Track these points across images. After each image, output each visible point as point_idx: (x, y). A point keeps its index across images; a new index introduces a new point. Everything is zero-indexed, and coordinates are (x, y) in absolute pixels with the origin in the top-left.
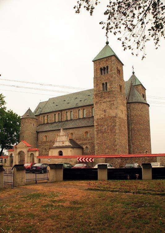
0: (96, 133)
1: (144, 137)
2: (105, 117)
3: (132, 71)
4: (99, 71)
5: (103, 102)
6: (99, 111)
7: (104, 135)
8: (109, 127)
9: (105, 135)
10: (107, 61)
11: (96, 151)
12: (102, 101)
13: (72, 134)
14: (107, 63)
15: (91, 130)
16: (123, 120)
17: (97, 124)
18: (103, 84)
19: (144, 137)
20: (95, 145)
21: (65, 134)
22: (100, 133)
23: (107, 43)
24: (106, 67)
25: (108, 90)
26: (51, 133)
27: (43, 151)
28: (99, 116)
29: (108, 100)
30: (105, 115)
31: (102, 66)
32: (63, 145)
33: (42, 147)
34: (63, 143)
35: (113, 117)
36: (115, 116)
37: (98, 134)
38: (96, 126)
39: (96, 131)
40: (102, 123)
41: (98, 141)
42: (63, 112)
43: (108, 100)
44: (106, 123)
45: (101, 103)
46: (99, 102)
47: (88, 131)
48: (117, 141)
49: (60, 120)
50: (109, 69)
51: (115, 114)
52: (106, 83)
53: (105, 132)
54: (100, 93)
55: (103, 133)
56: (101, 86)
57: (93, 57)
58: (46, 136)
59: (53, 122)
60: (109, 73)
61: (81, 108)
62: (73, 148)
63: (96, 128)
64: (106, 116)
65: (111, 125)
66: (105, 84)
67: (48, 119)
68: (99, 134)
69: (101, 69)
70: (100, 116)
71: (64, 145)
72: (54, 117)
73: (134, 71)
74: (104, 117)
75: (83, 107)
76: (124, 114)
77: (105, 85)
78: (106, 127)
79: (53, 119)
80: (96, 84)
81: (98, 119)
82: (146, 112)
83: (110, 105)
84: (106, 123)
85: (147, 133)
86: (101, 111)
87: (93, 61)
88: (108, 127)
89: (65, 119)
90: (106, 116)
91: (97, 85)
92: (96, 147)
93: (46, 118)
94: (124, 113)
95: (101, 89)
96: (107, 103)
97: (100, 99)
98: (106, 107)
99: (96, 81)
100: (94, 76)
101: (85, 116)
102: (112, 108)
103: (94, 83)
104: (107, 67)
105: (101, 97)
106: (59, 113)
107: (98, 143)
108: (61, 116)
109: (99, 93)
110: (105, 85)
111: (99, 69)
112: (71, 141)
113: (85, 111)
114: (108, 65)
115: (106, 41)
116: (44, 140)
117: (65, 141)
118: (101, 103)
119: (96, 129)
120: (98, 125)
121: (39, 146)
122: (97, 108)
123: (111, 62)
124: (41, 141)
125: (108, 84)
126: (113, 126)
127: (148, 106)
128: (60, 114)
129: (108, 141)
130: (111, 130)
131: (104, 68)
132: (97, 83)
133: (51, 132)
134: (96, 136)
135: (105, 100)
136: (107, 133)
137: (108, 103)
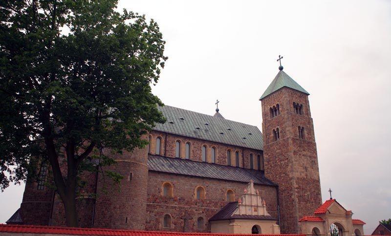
9: (308, 204)
10: (300, 97)
15: (264, 191)
17: (297, 186)
18: (299, 127)
23: (281, 68)
26: (182, 181)
29: (309, 154)
30: (306, 175)
33: (156, 210)
38: (297, 188)
42: (170, 139)
55: (306, 202)
61: (209, 144)
65: (314, 191)
74: (305, 177)
75: (215, 144)
77: (301, 130)
88: (311, 194)
105: (300, 146)
108: (166, 144)
110: (301, 130)
116: (162, 194)
117: (260, 206)
119: (297, 194)
124: (153, 196)
126: (317, 194)
133: (183, 177)
135: (305, 153)
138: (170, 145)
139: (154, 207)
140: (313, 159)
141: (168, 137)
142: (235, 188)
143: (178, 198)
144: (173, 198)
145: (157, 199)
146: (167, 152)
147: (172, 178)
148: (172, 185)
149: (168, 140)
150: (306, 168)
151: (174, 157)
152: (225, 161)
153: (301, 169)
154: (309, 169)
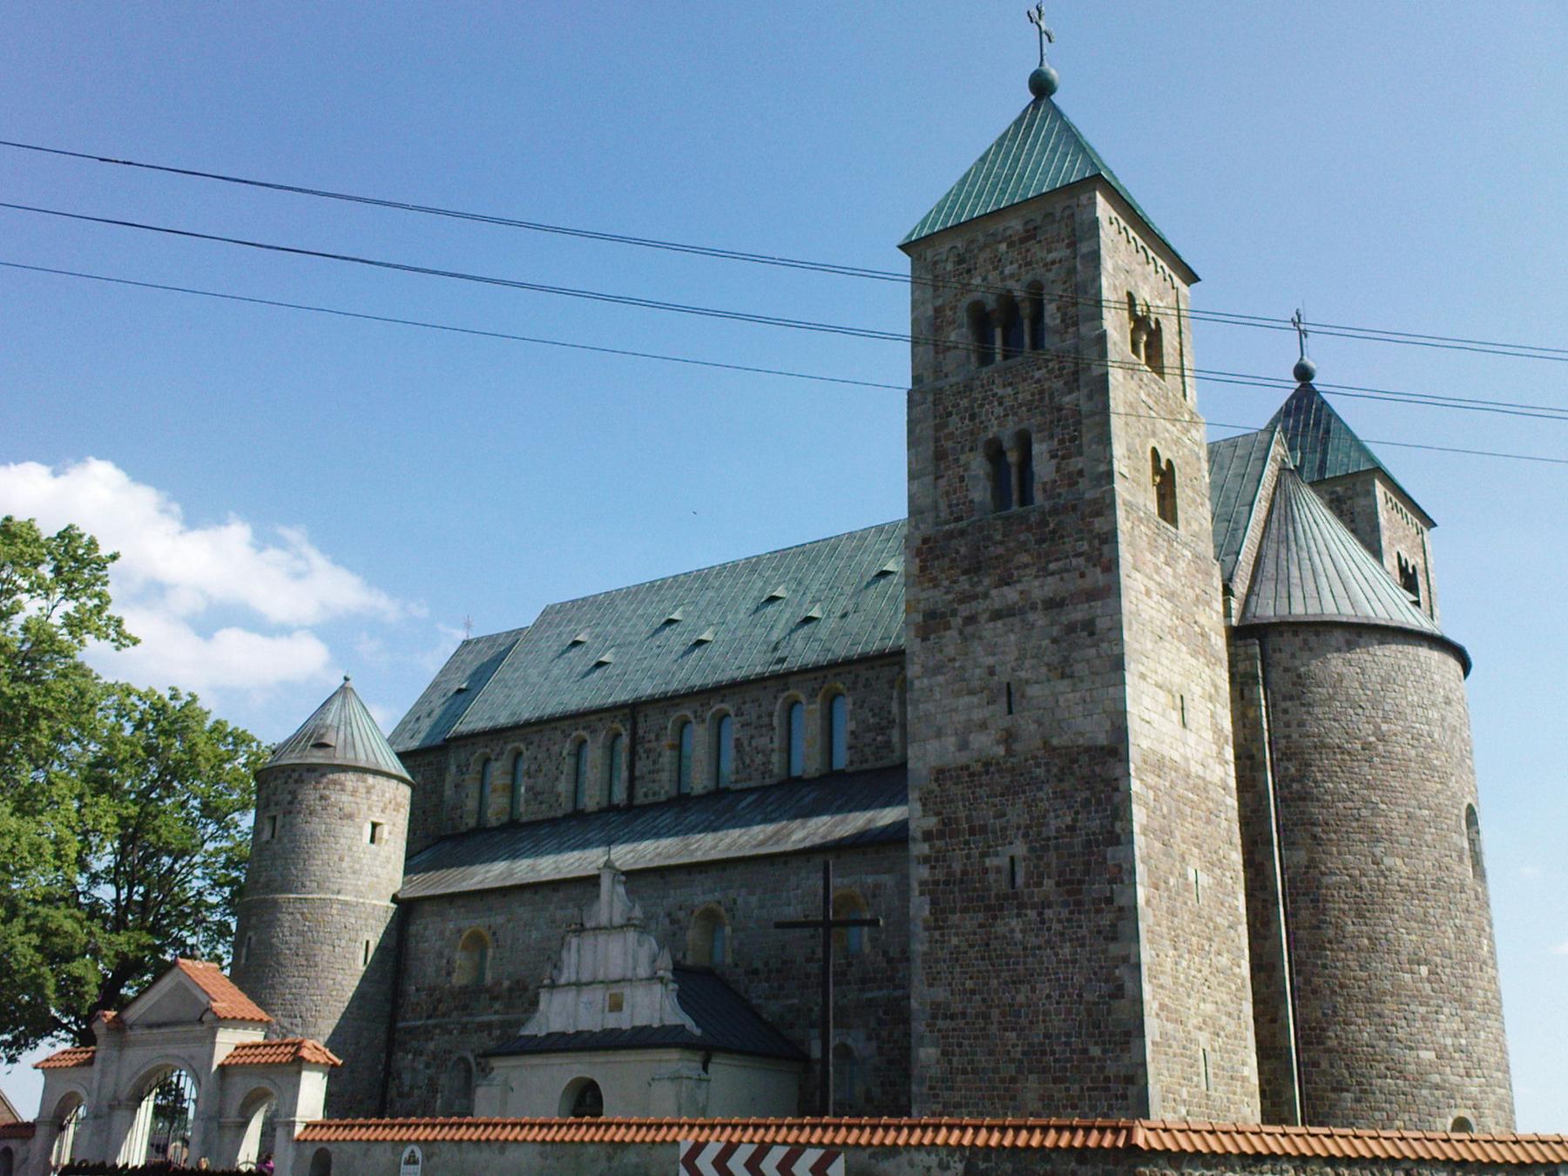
0: (920, 907)
1: (1424, 970)
2: (1010, 752)
3: (1296, 361)
4: (959, 335)
5: (997, 615)
6: (958, 694)
7: (1000, 928)
8: (1045, 848)
9: (1012, 925)
11: (925, 1090)
12: (981, 606)
13: (711, 918)
14: (1038, 251)
16: (1202, 787)
17: (932, 822)
19: (1424, 970)
20: (919, 1027)
21: (638, 913)
22: (965, 910)
23: (1041, 86)
24: (1019, 293)
25: (1039, 497)
27: (443, 1080)
28: (951, 741)
29: (1040, 589)
30: (1009, 737)
31: (985, 285)
32: (612, 1021)
33: (431, 1046)
34: (616, 1006)
35: (1088, 750)
36: (1102, 740)
37: (938, 922)
38: (928, 836)
39: (931, 889)
40: (985, 815)
41: (941, 994)
43: (1040, 589)
44: (1016, 814)
45: (971, 620)
46: (954, 613)
47: (857, 890)
48: (1129, 985)
49: (620, 796)
50: (1050, 309)
51: (1108, 726)
52: (1024, 441)
53: (1013, 899)
54: (962, 533)
55: (994, 911)
56: (978, 465)
57: (910, 219)
58: (477, 942)
59: (560, 814)
60: (1051, 342)
62: (706, 1050)
63: (926, 860)
64: (1018, 747)
65: (1071, 828)
66: (1007, 443)
67: (513, 789)
68: (955, 918)
69: (981, 320)
70: (963, 746)
71: (623, 1021)
72: (570, 761)
73: (1310, 363)
74: (1001, 751)
76: (1209, 735)
78: (1020, 849)
79: (563, 786)
80: (928, 449)
81: (940, 774)
82: (1434, 714)
83: (1055, 641)
84: (1016, 814)
85: (1460, 931)
86: (975, 700)
87: (900, 247)
88: (1038, 851)
89: (663, 785)
90: (1018, 747)
91: (940, 456)
92: (927, 1054)
93: (498, 773)
94: (1199, 713)
95: (980, 493)
96: (1031, 617)
97: (964, 584)
98: (1021, 658)
99: (927, 429)
100: (916, 379)
101: (841, 760)
102: (1080, 669)
103: (913, 442)
104: (1036, 292)
105: (975, 568)
106: (618, 735)
107: (938, 1011)
108: (633, 753)
109: (950, 535)
111: (963, 316)
112: (692, 981)
113: (844, 707)
114: (1039, 271)
115: (1036, 67)
118: (971, 620)
119: (924, 872)
120: (941, 835)
121: (410, 1031)
122: (938, 670)
123: (1072, 245)
124: (431, 990)
125: (1039, 449)
126: (1088, 844)
127: (1453, 665)
128: (625, 740)
129: (1044, 988)
130: (1072, 887)
131: (1008, 303)
132: (937, 440)
134: (919, 947)
135: (1011, 595)
136: (1032, 914)
137: (1039, 619)
138: (648, 751)
139: (427, 1033)
140: (1078, 614)
141: (641, 719)
142: (732, 894)
143: (506, 984)
144: (488, 991)
145: (440, 1001)
146: (638, 784)
147: (490, 909)
148: (488, 937)
149: (641, 732)
150: (1010, 695)
151: (663, 798)
152: (888, 744)
153: (971, 708)
154: (1034, 691)
